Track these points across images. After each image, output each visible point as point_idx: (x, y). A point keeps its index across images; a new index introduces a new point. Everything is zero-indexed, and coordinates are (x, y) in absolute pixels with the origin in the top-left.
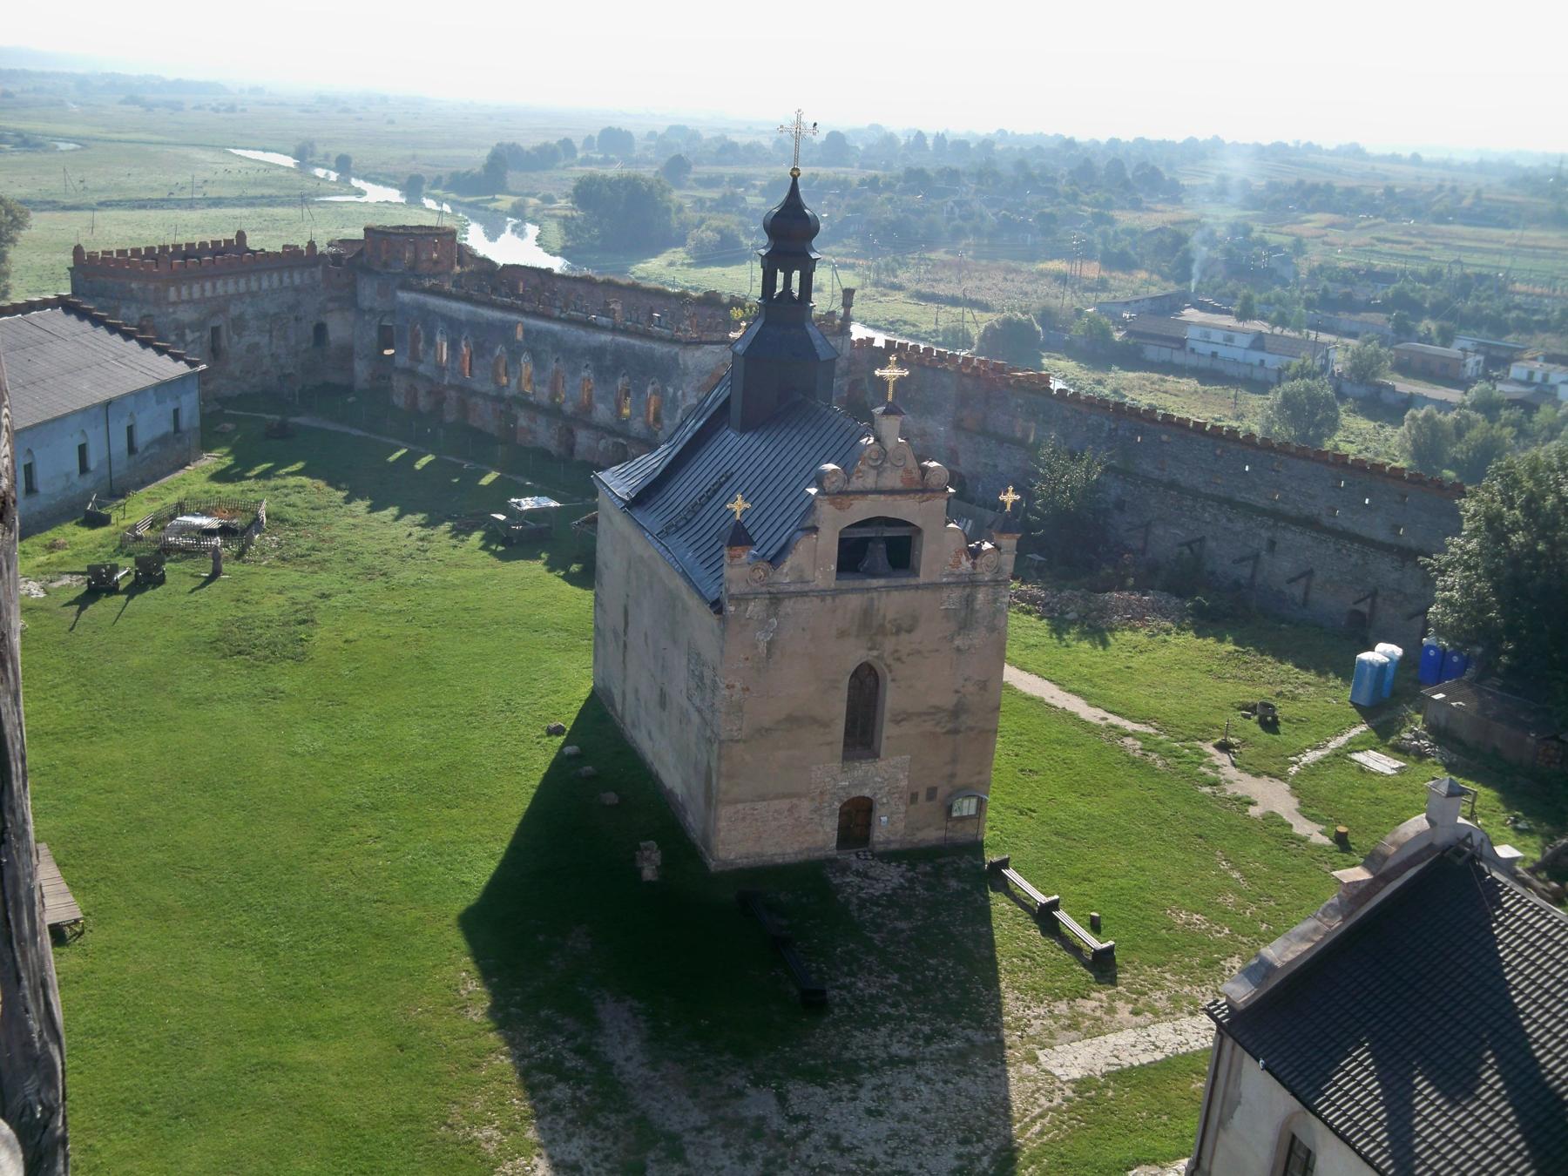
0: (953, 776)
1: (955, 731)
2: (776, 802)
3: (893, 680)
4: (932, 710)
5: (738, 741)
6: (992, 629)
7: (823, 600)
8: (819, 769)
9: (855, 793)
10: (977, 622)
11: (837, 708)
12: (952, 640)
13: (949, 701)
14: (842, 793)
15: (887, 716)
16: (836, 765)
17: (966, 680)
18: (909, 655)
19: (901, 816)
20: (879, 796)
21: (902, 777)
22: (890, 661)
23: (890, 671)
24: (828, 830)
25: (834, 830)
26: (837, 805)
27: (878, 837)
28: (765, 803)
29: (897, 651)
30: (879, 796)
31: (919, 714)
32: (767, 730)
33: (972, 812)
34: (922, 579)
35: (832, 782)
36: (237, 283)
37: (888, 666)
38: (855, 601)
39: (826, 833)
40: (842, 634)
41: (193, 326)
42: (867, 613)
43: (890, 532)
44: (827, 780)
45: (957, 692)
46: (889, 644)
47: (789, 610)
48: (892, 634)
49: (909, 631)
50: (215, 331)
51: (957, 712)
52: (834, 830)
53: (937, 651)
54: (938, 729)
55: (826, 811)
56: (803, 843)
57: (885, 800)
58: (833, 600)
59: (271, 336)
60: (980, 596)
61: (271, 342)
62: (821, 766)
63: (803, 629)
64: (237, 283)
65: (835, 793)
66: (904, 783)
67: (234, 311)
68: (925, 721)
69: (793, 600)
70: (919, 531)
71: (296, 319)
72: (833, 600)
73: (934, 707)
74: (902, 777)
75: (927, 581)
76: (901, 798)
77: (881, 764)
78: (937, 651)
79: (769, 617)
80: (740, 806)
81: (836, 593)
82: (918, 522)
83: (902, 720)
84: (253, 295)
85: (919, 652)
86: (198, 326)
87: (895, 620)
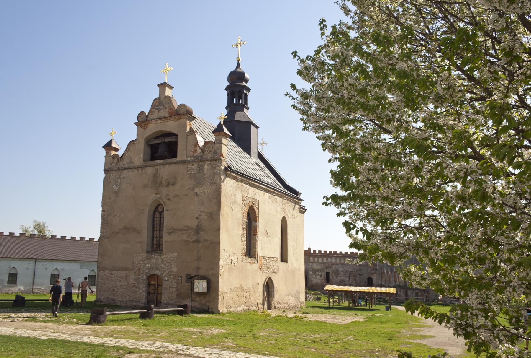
0: (198, 268)
1: (198, 241)
2: (119, 272)
3: (167, 210)
4: (186, 228)
5: (105, 237)
6: (213, 183)
7: (138, 170)
8: (137, 256)
9: (153, 272)
10: (205, 180)
11: (144, 223)
12: (194, 189)
13: (194, 224)
14: (147, 271)
15: (165, 229)
16: (144, 255)
17: (201, 212)
18: (173, 197)
19: (174, 289)
20: (163, 275)
21: (174, 266)
22: (165, 200)
23: (165, 205)
24: (141, 291)
25: (143, 292)
26: (145, 277)
27: (164, 300)
28: (115, 271)
29: (168, 195)
30: (163, 275)
31: (180, 230)
32: (116, 233)
33: (205, 291)
34: (179, 158)
35: (143, 264)
36: (336, 260)
37: (164, 203)
38: (150, 170)
39: (140, 293)
40: (145, 186)
41: (318, 270)
42: (155, 176)
43: (167, 140)
44: (141, 263)
45: (197, 218)
46: (164, 191)
47: (125, 175)
48: (165, 186)
49: (173, 185)
50: (328, 274)
51: (198, 230)
52: (143, 292)
53: (186, 195)
54: (189, 239)
55: (140, 281)
56: (130, 297)
57: (166, 279)
58: (142, 170)
59: (349, 278)
60: (206, 166)
61: (349, 280)
62: (138, 255)
63: (130, 184)
64: (336, 260)
65: (144, 271)
66: (175, 270)
67: (334, 267)
68: (183, 234)
69: (126, 171)
70: (176, 135)
71: (360, 274)
72: (142, 170)
73: (187, 226)
74: (174, 266)
75: (181, 159)
76: (174, 278)
77: (163, 257)
78: (186, 195)
79: (118, 178)
80: (106, 272)
81: (143, 167)
82: (175, 132)
83: (172, 232)
84: (342, 264)
85: (177, 196)
86: (321, 270)
87: (167, 179)
